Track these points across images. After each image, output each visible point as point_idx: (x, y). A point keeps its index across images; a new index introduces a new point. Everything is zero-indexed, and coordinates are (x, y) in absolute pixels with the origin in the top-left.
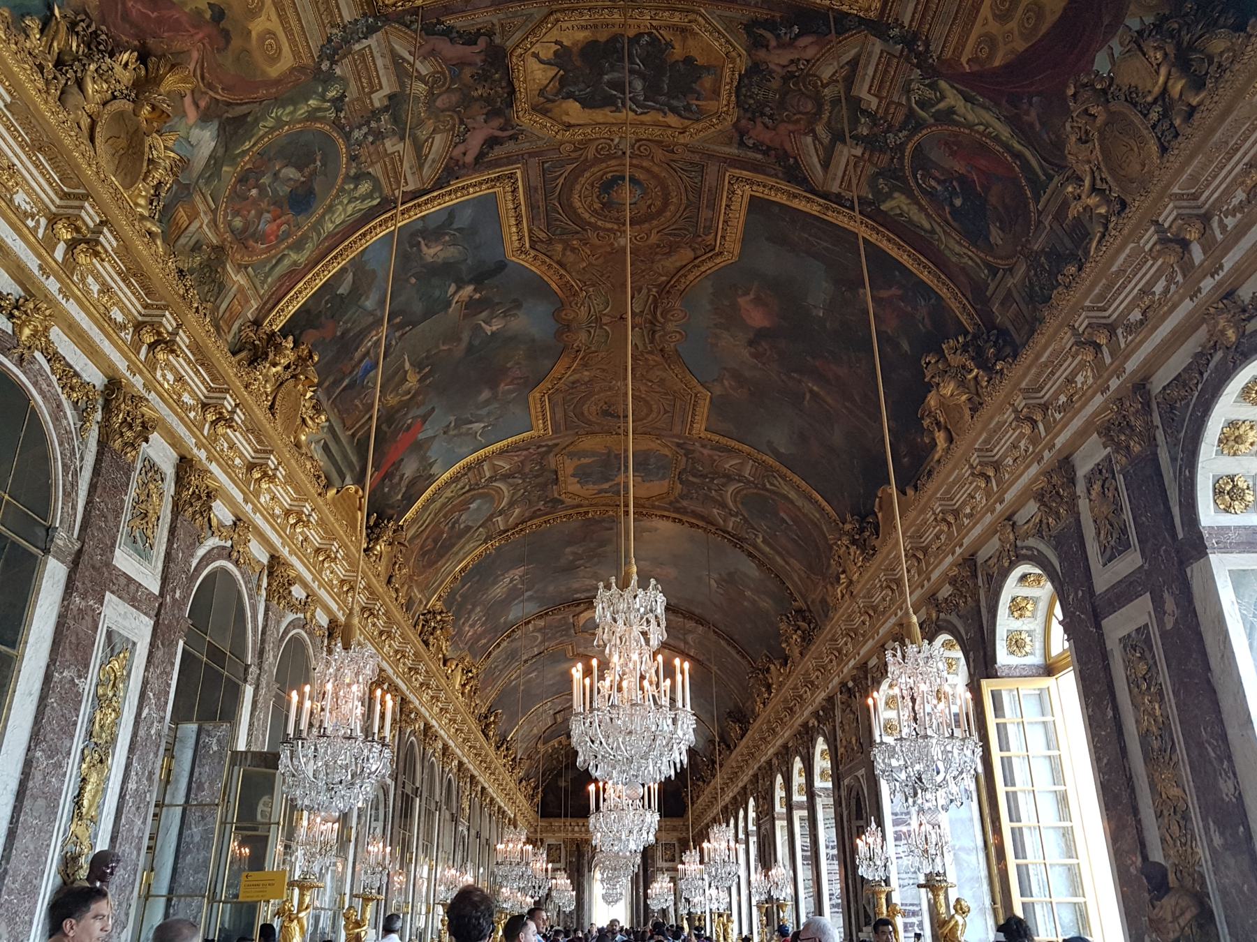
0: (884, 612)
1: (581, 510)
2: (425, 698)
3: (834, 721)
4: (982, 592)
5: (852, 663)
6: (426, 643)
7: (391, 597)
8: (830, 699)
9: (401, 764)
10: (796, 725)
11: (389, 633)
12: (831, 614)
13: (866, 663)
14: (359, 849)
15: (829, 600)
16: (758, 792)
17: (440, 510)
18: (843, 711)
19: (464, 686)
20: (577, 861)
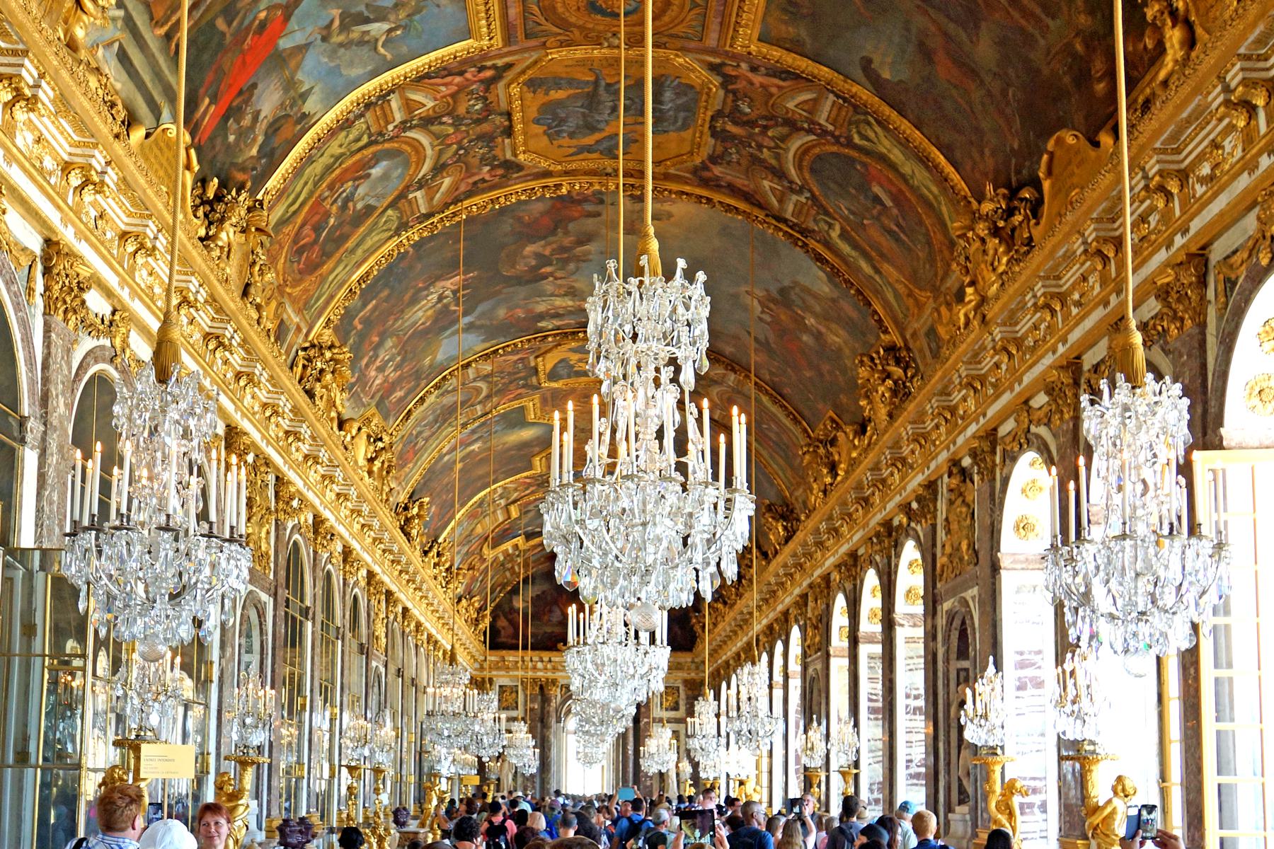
0: (1033, 349)
1: (551, 182)
2: (314, 477)
3: (935, 517)
4: (1212, 313)
5: (973, 428)
6: (310, 394)
7: (248, 317)
8: (931, 486)
9: (282, 573)
10: (873, 523)
11: (250, 376)
12: (945, 351)
13: (995, 429)
14: (226, 693)
15: (942, 331)
16: (806, 619)
17: (322, 178)
18: (951, 502)
19: (371, 460)
20: (542, 710)
